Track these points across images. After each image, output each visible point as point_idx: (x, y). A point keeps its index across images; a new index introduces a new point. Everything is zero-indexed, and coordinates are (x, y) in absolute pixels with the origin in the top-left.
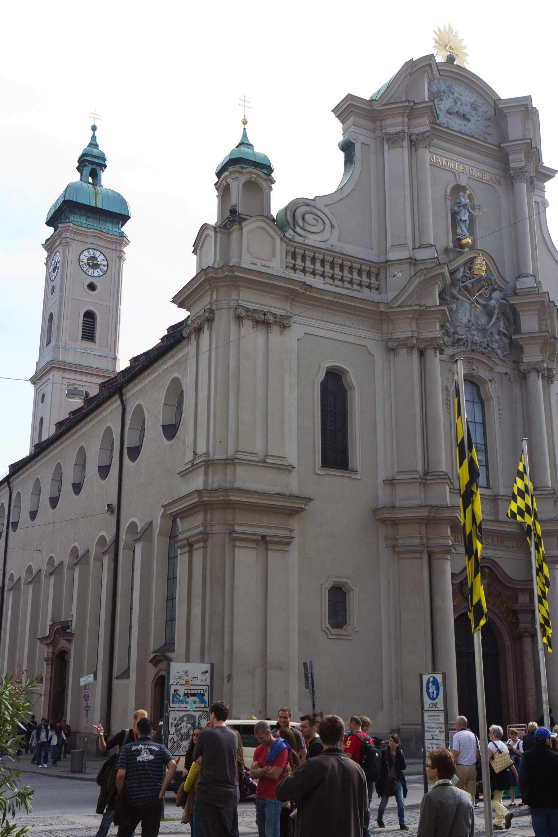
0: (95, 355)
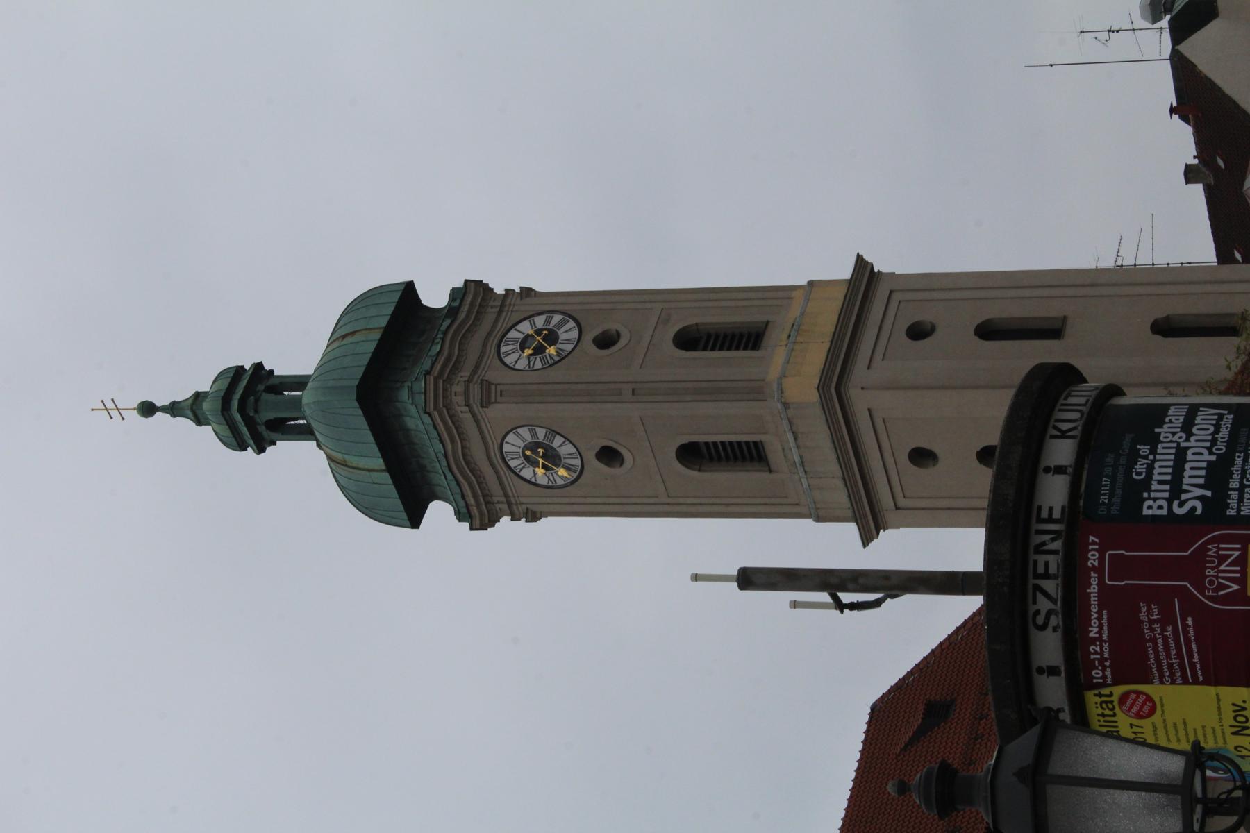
0: (798, 447)
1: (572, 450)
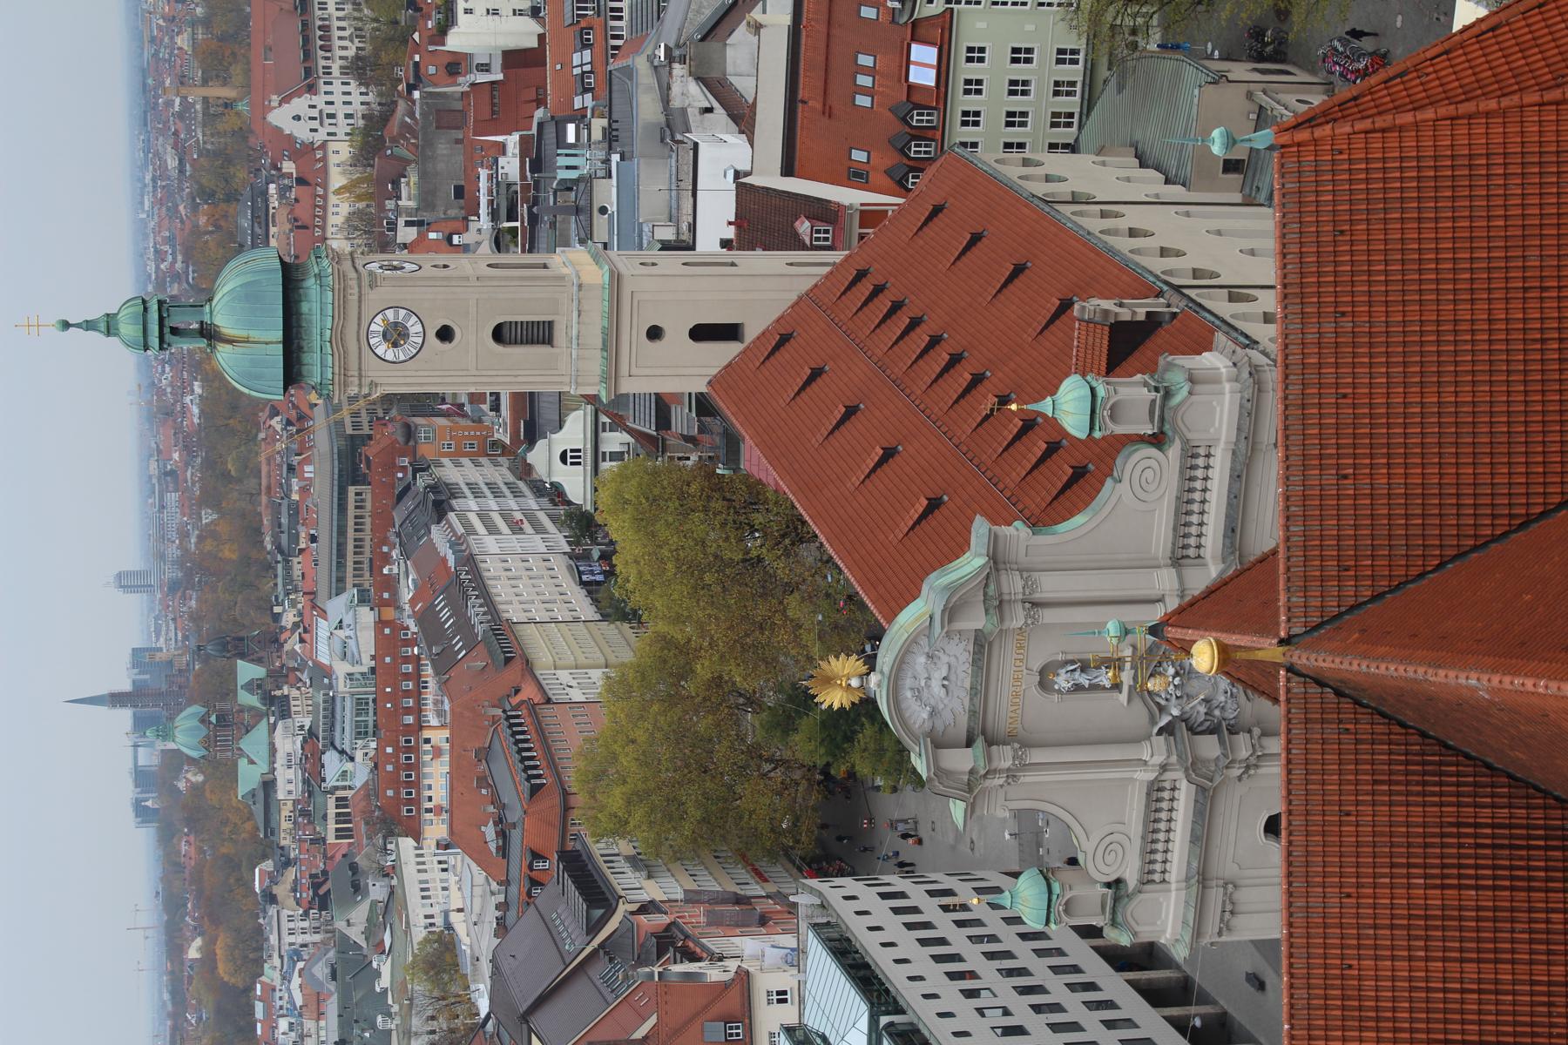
1: (419, 328)
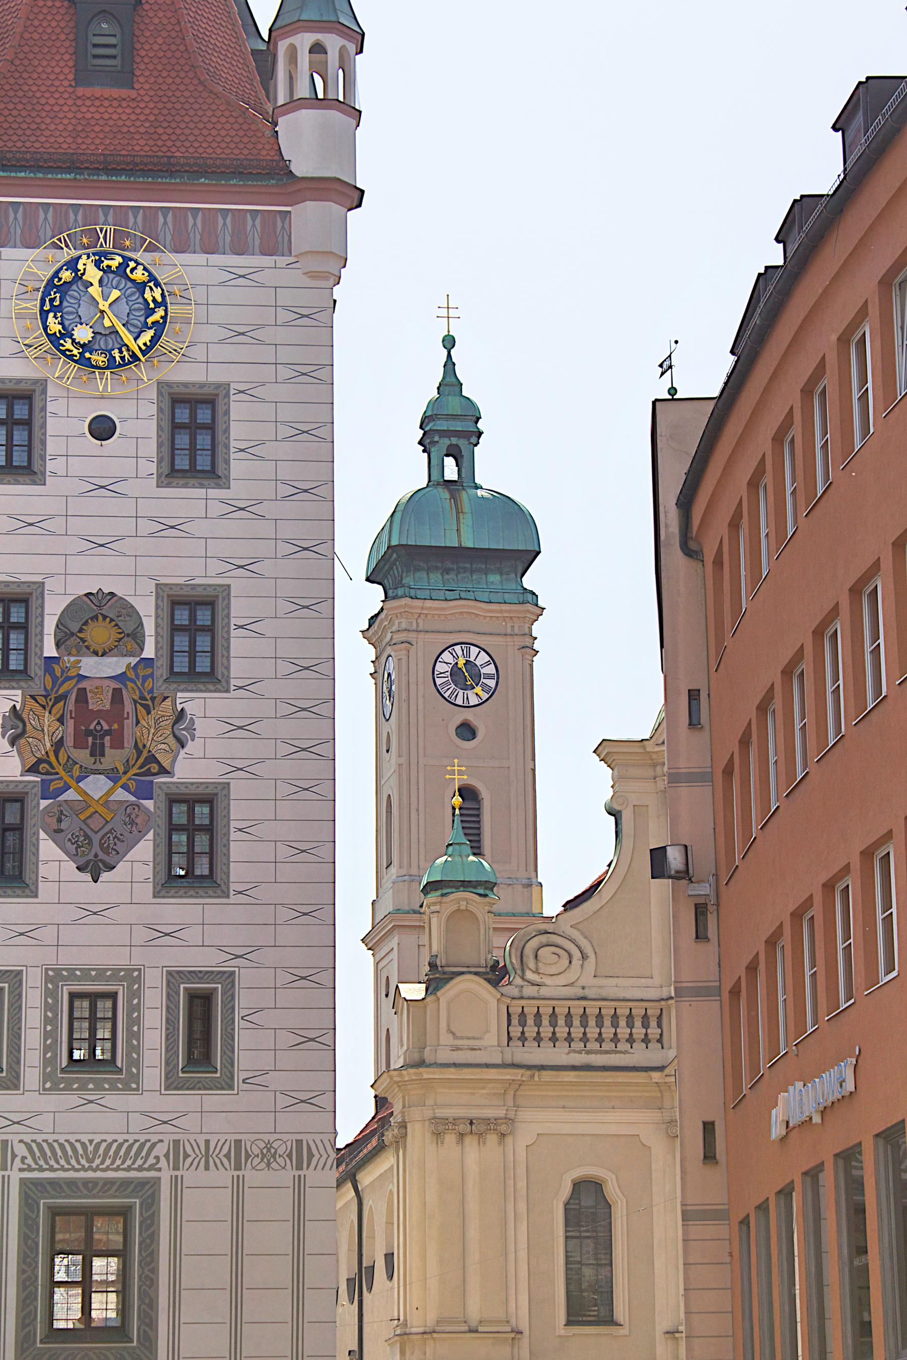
1: (474, 701)
